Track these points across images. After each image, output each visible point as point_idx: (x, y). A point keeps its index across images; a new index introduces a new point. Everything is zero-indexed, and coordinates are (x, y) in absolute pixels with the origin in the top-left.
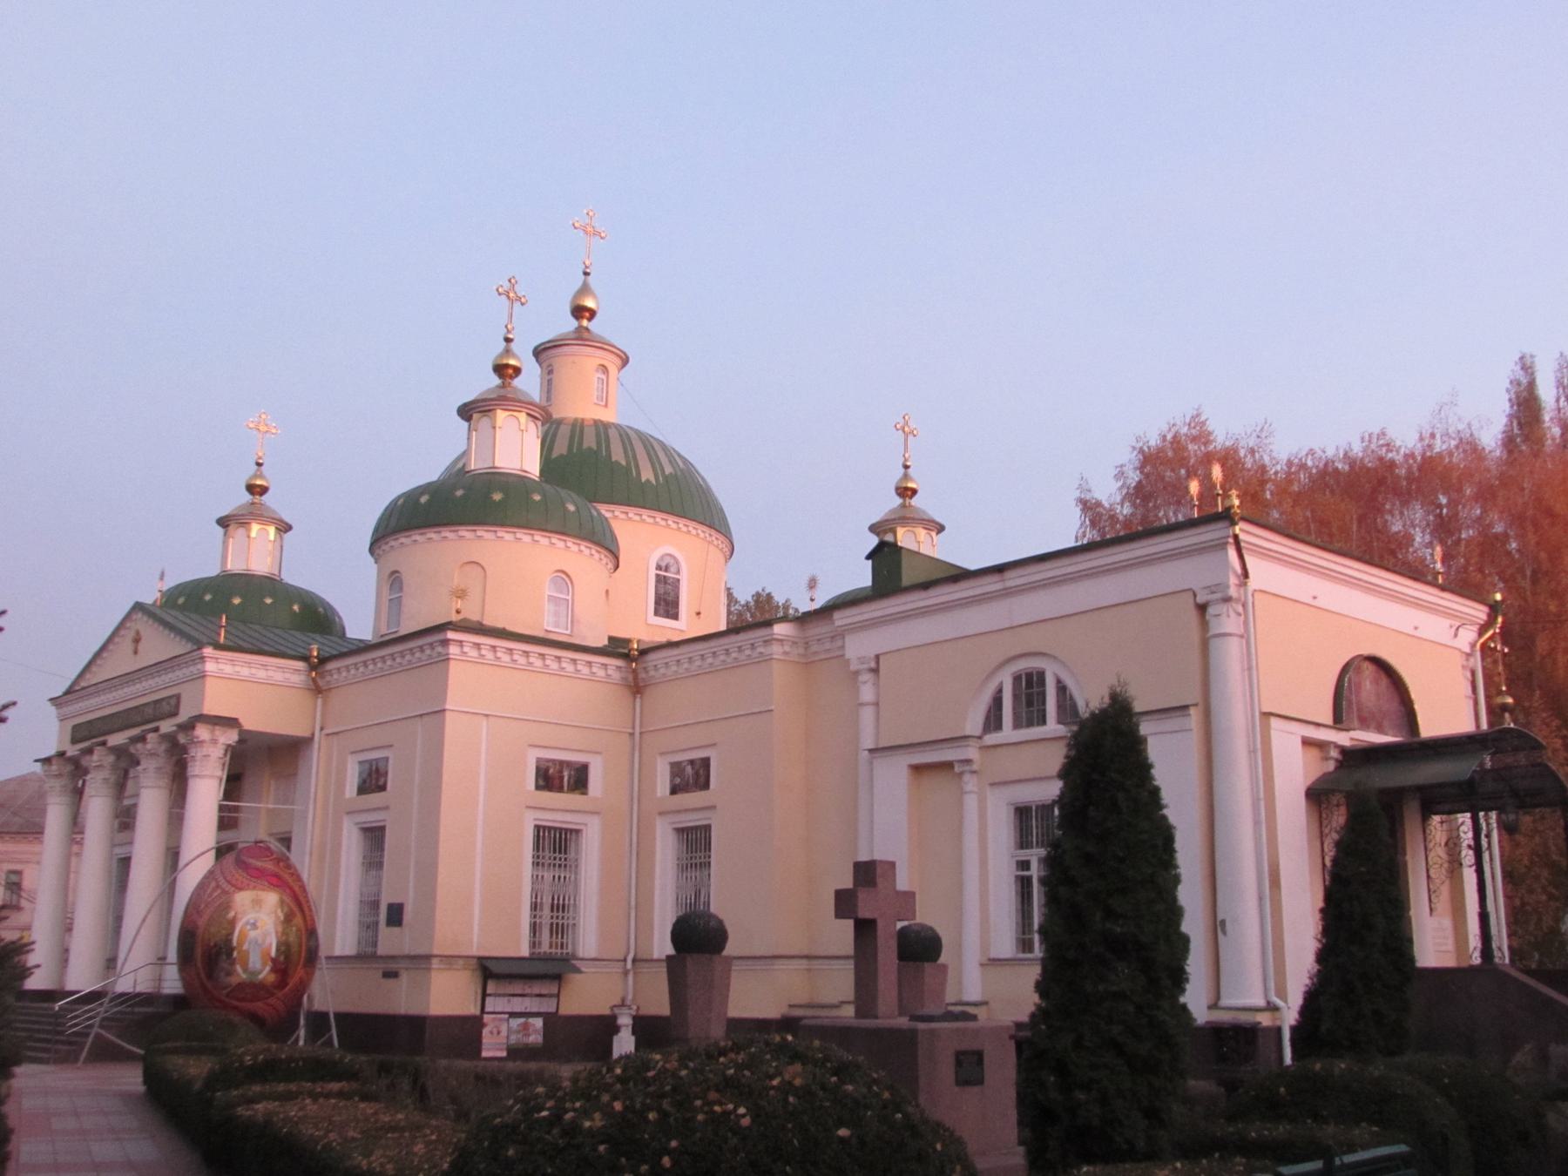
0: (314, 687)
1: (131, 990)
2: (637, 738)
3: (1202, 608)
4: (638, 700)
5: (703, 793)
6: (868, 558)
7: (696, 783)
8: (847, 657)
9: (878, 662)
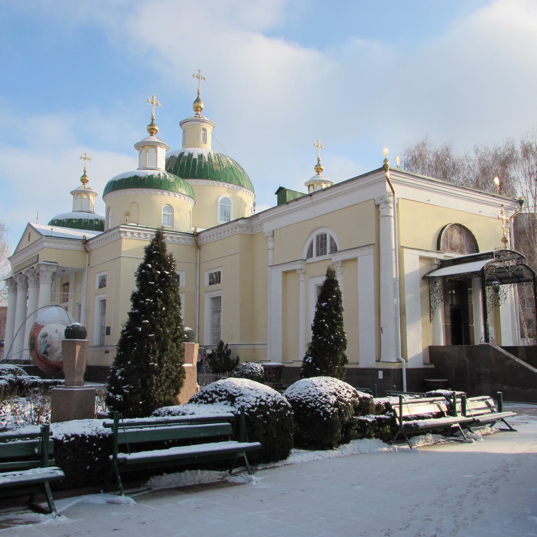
0: (85, 250)
1: (19, 359)
2: (198, 265)
3: (378, 206)
4: (199, 251)
5: (219, 284)
6: (276, 194)
7: (217, 280)
8: (264, 232)
9: (274, 233)
